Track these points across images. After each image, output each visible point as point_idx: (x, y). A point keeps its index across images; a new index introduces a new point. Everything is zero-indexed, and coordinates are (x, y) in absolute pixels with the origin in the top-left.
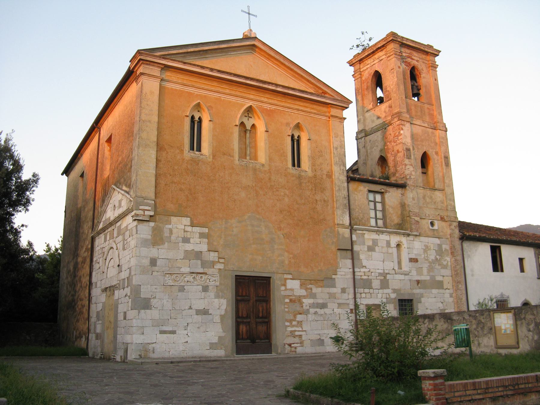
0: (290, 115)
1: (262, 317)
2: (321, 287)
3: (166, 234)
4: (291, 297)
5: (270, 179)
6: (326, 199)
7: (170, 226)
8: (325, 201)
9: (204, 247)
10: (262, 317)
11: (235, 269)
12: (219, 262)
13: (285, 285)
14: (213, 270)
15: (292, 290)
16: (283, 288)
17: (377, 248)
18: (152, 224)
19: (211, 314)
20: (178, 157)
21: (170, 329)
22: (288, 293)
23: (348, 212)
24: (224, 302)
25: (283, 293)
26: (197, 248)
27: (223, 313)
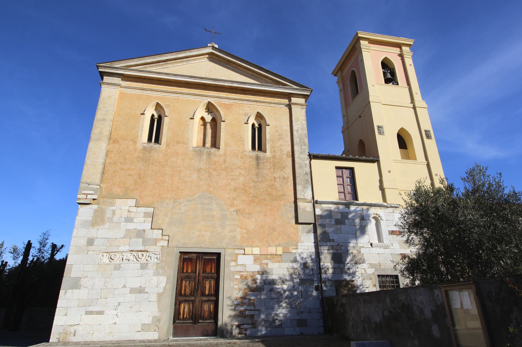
0: (249, 107)
1: (208, 295)
2: (279, 262)
3: (108, 214)
4: (242, 273)
5: (225, 161)
6: (286, 176)
7: (114, 208)
8: (284, 178)
9: (147, 226)
10: (208, 295)
11: (180, 245)
12: (162, 239)
13: (235, 261)
14: (155, 247)
15: (244, 265)
16: (233, 264)
17: (347, 221)
18: (95, 207)
19: (147, 293)
20: (131, 148)
21: (99, 309)
22: (239, 269)
23: (311, 186)
24: (163, 280)
25: (232, 269)
26: (140, 227)
27: (161, 291)
